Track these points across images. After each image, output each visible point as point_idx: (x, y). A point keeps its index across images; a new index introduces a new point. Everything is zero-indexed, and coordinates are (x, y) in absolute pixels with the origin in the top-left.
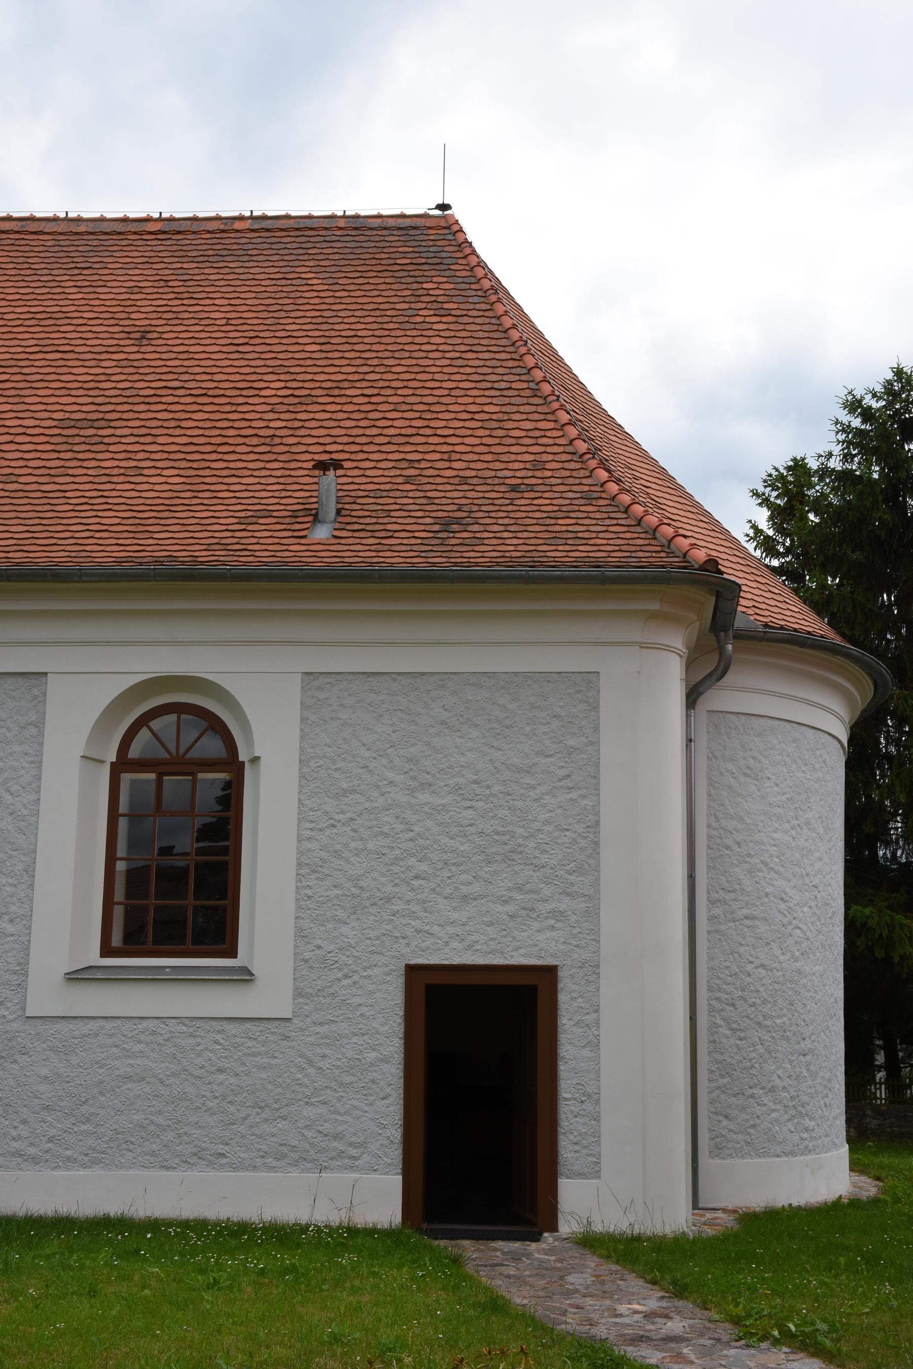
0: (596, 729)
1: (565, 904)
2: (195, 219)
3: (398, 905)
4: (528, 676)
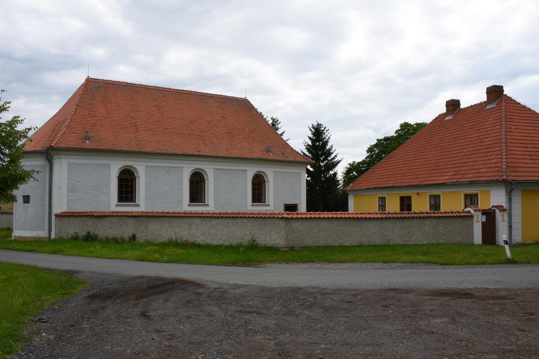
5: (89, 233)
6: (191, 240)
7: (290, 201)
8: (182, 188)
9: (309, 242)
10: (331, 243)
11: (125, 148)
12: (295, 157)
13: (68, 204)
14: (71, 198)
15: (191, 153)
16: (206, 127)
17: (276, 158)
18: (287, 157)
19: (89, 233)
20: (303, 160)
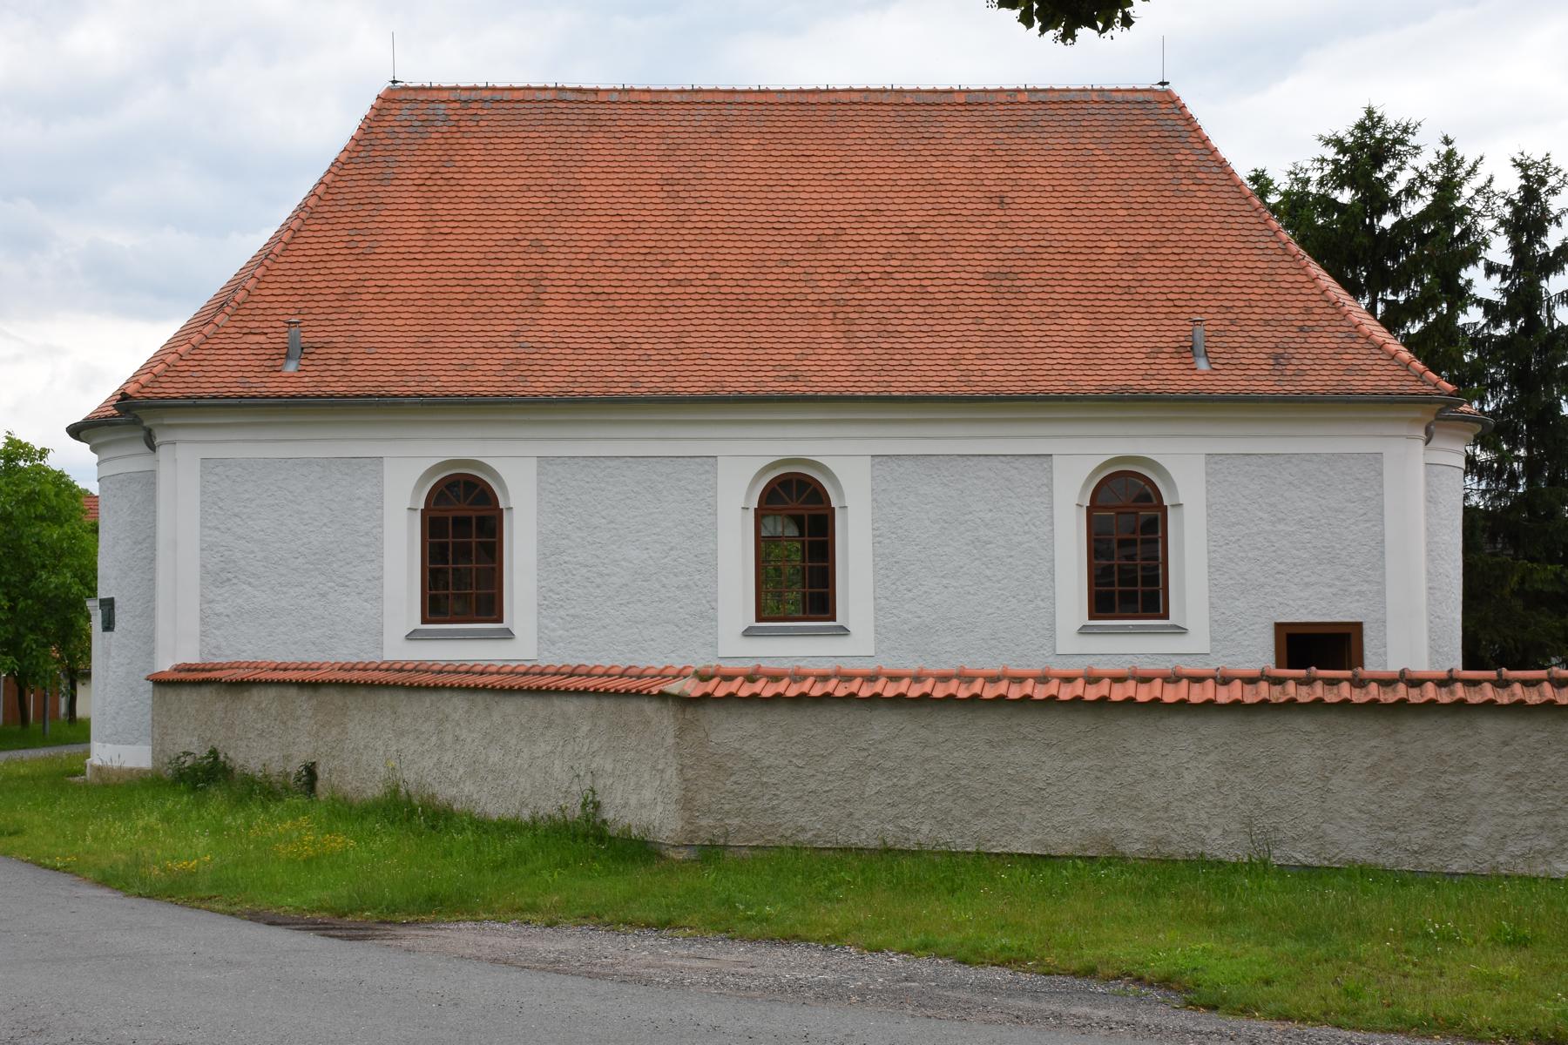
0: (1381, 486)
1: (1365, 587)
2: (985, 91)
3: (1268, 589)
4: (1341, 455)
5: (214, 753)
6: (445, 793)
7: (1315, 607)
8: (715, 552)
9: (807, 821)
10: (925, 832)
11: (452, 383)
12: (1349, 369)
13: (203, 634)
14: (219, 608)
15: (748, 388)
16: (889, 256)
17: (1234, 383)
18: (1301, 373)
19: (214, 753)
20: (1394, 387)
